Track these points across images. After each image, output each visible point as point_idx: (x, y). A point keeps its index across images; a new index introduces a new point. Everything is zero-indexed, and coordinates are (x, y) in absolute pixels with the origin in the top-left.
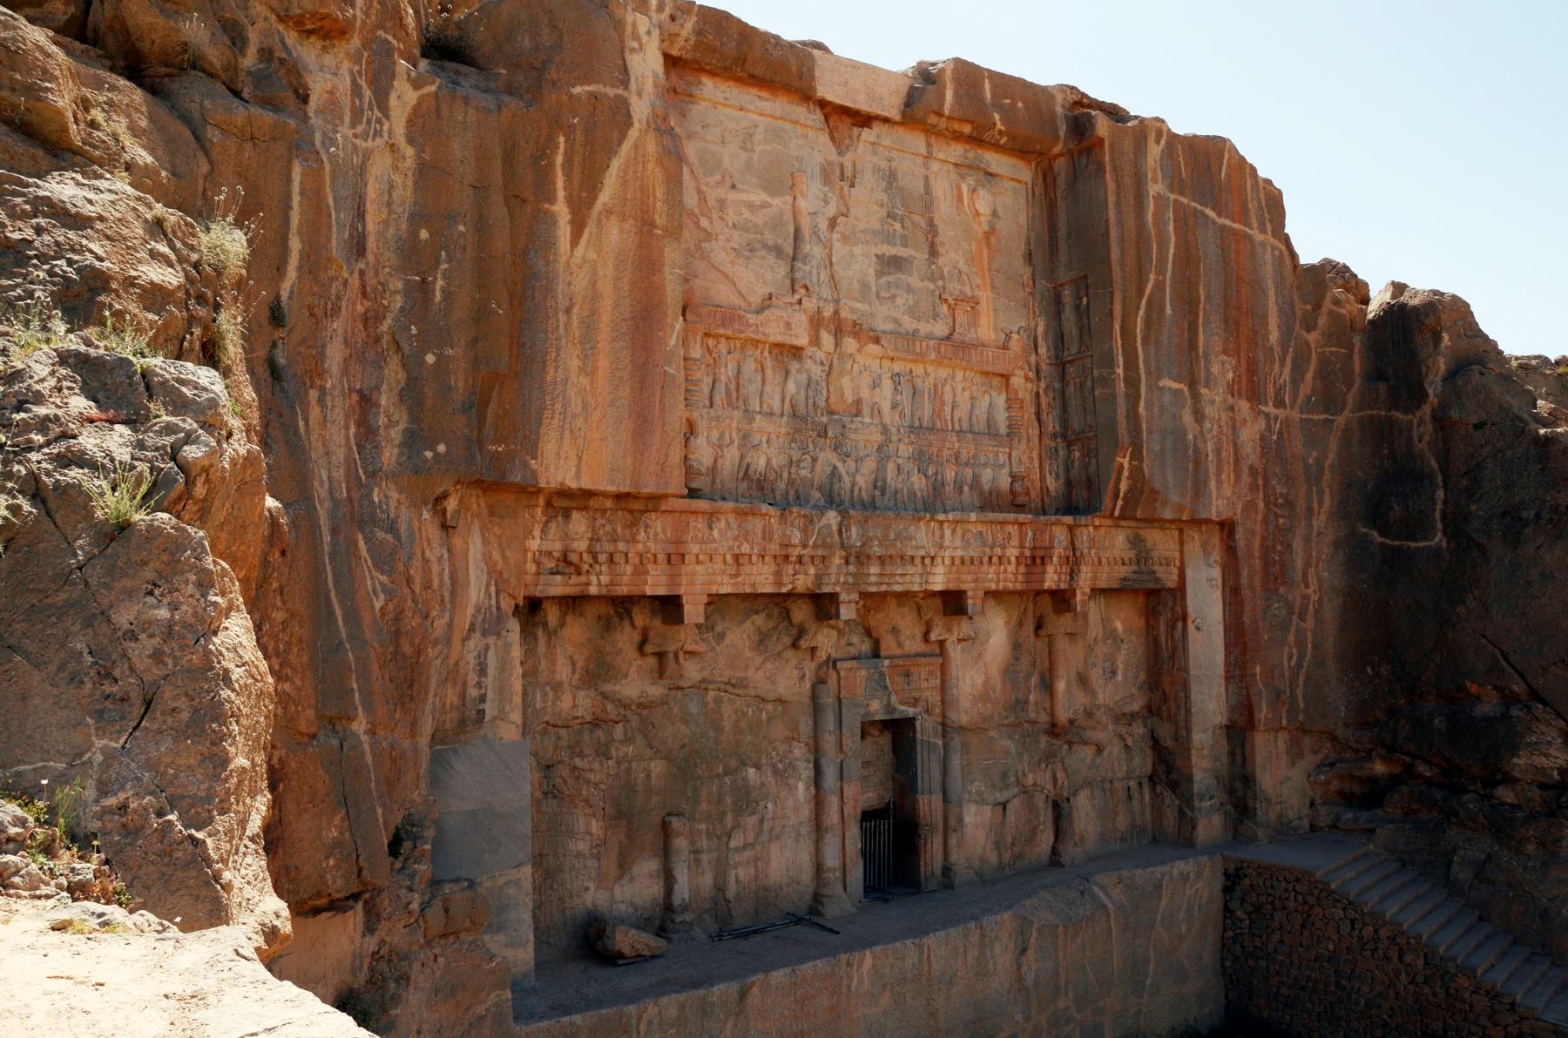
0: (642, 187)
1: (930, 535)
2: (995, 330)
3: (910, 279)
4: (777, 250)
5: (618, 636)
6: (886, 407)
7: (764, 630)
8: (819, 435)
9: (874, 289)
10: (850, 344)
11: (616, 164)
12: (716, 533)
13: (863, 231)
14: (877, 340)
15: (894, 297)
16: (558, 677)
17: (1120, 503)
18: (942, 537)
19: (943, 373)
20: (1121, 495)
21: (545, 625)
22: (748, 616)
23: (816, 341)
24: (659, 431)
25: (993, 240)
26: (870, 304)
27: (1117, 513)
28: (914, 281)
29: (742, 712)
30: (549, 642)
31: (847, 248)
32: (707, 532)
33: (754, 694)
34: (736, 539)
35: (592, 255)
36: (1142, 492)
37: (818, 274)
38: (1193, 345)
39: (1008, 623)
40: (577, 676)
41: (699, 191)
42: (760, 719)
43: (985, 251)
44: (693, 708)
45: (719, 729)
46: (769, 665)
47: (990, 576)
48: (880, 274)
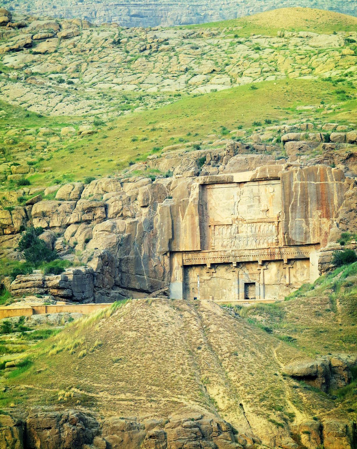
6: (248, 231)
10: (240, 222)
17: (287, 243)
38: (306, 210)
48: (248, 209)
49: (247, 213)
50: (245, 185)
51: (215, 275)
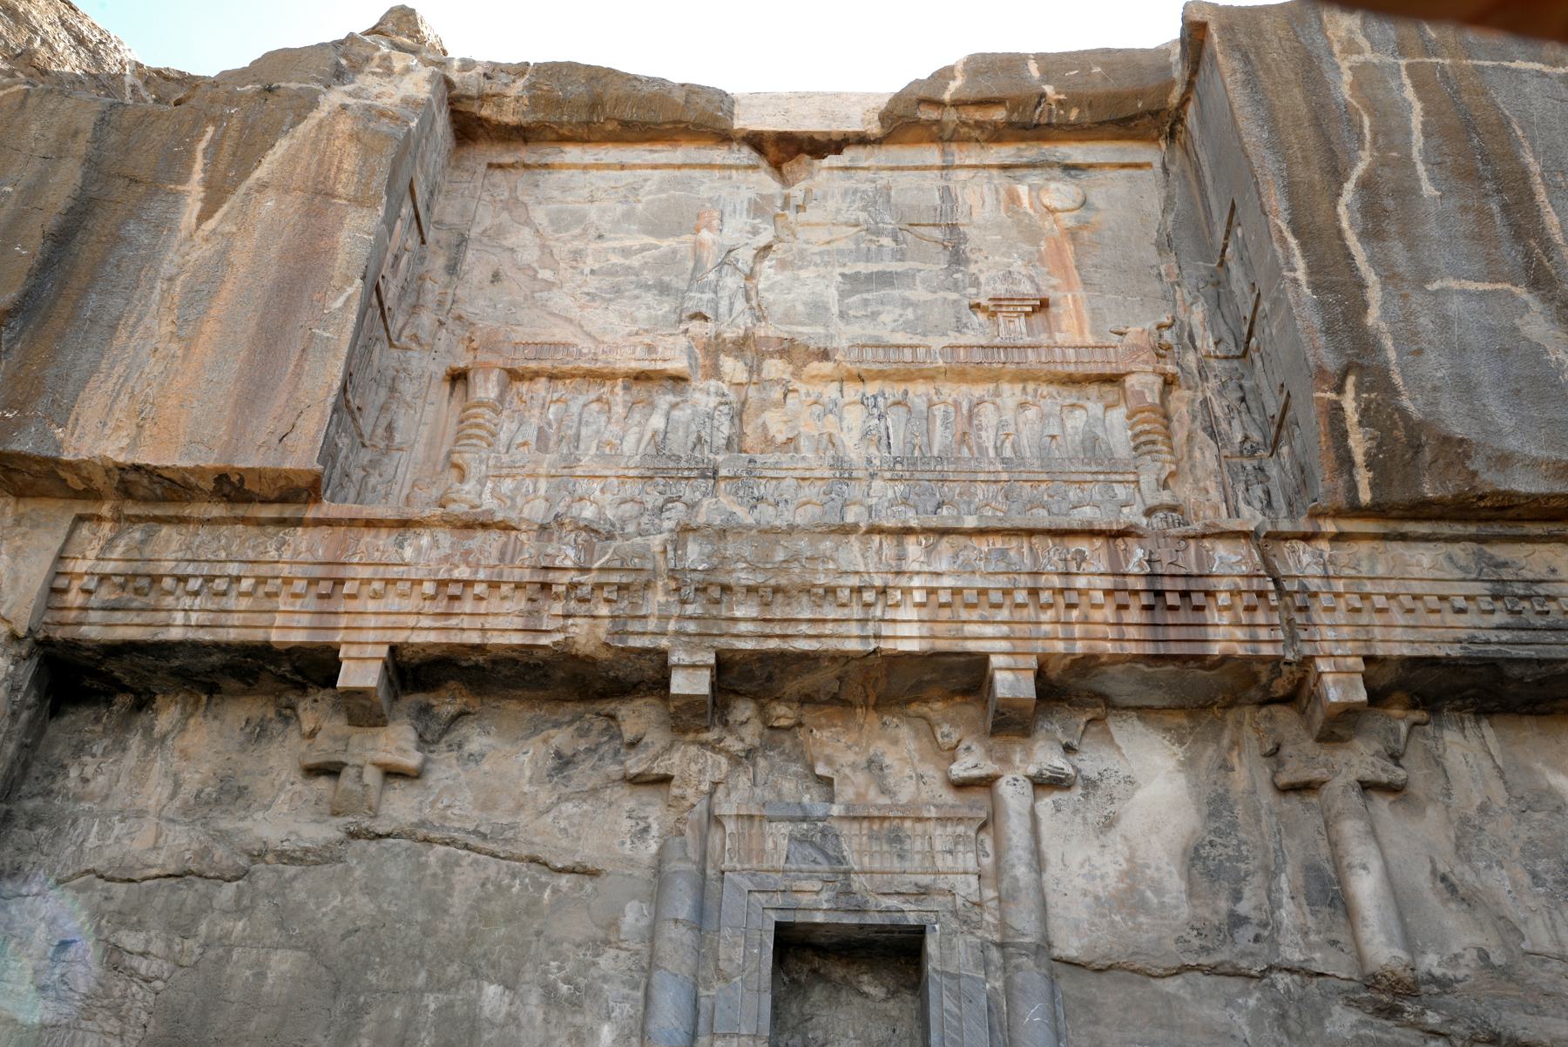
0: (320, 163)
1: (871, 554)
2: (1095, 332)
3: (908, 293)
4: (663, 289)
5: (274, 748)
7: (568, 752)
8: (705, 477)
9: (835, 310)
10: (774, 368)
11: (282, 146)
12: (408, 553)
13: (820, 253)
14: (825, 355)
15: (874, 316)
16: (140, 802)
17: (1363, 478)
18: (901, 557)
19: (979, 391)
20: (1359, 458)
21: (148, 731)
22: (536, 731)
23: (715, 372)
24: (284, 396)
25: (1085, 234)
26: (826, 326)
27: (1365, 496)
28: (919, 293)
29: (499, 887)
30: (146, 753)
31: (788, 273)
32: (392, 549)
33: (525, 852)
34: (446, 558)
35: (229, 228)
36: (1417, 448)
37: (732, 304)
39: (1189, 764)
40: (177, 803)
41: (543, 247)
42: (536, 902)
43: (1069, 248)
44: (394, 871)
45: (437, 907)
46: (569, 808)
47: (1046, 628)
48: (843, 295)
49: (842, 315)
50: (832, 160)
51: (401, 806)
